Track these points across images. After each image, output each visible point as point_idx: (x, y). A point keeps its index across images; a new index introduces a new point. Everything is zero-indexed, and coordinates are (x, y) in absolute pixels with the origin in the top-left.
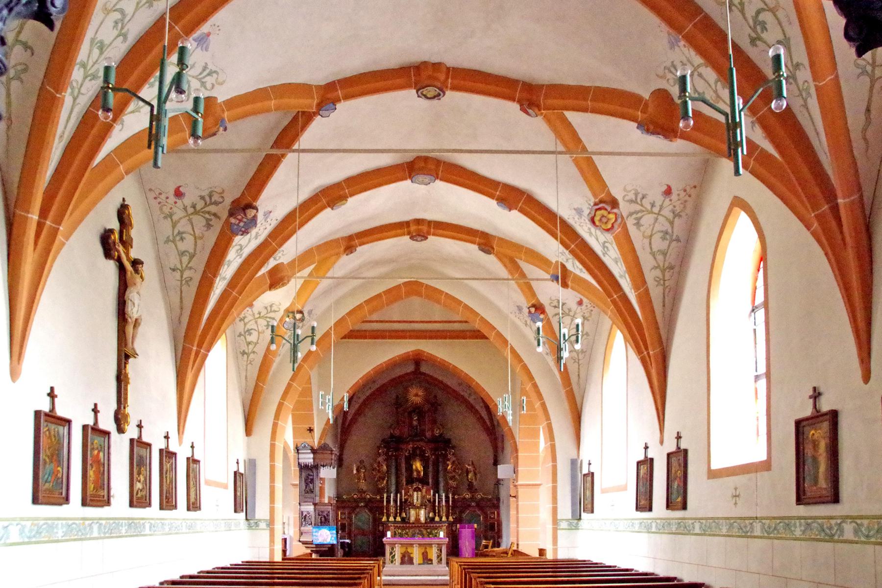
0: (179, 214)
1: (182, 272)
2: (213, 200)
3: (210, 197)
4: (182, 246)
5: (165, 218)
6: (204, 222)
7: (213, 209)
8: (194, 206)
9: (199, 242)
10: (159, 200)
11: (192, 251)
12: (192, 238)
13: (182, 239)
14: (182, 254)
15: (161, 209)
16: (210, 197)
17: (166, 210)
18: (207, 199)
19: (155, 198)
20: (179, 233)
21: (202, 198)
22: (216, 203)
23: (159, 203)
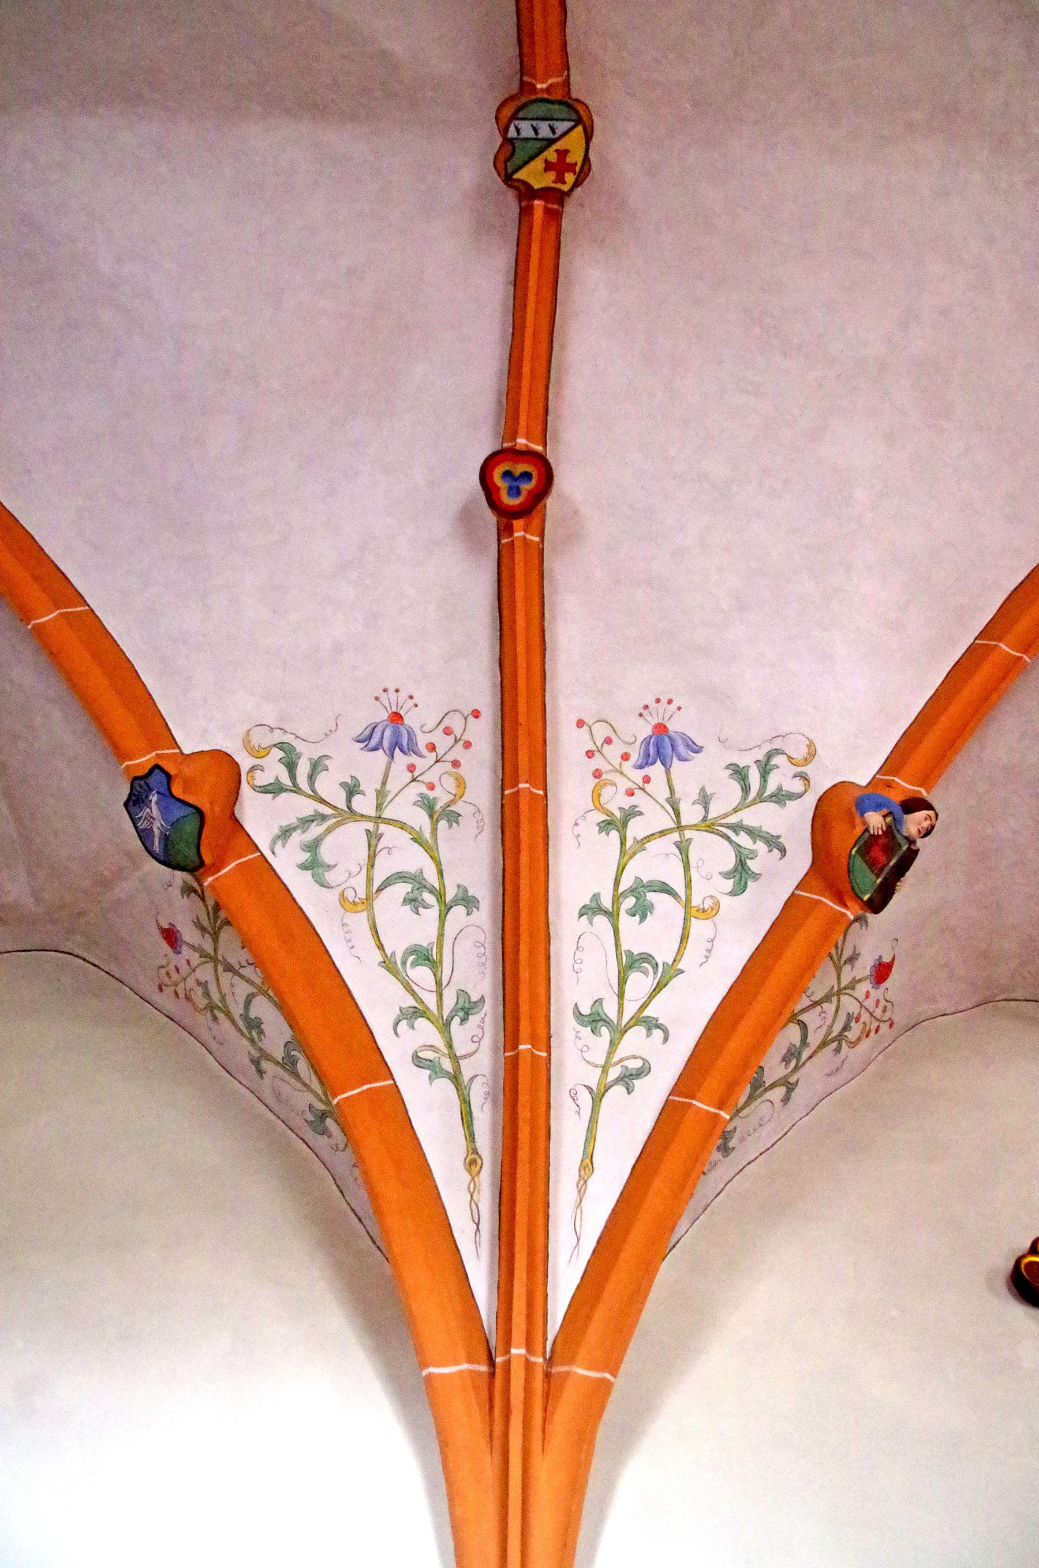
0: (654, 817)
1: (619, 1032)
2: (771, 788)
3: (765, 774)
4: (636, 935)
5: (606, 826)
6: (730, 862)
7: (764, 816)
8: (705, 800)
9: (696, 925)
10: (597, 762)
11: (664, 955)
12: (679, 911)
13: (642, 911)
14: (630, 963)
15: (596, 795)
16: (765, 774)
17: (616, 801)
18: (754, 778)
19: (590, 754)
20: (639, 889)
21: (740, 774)
22: (780, 797)
23: (597, 774)
